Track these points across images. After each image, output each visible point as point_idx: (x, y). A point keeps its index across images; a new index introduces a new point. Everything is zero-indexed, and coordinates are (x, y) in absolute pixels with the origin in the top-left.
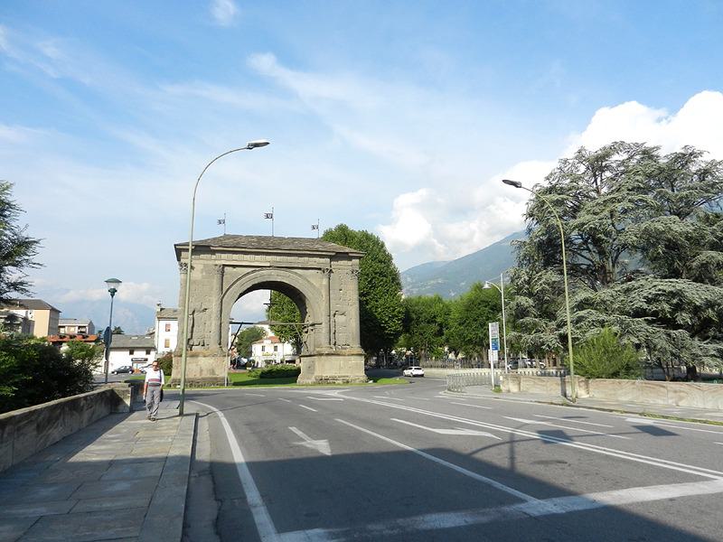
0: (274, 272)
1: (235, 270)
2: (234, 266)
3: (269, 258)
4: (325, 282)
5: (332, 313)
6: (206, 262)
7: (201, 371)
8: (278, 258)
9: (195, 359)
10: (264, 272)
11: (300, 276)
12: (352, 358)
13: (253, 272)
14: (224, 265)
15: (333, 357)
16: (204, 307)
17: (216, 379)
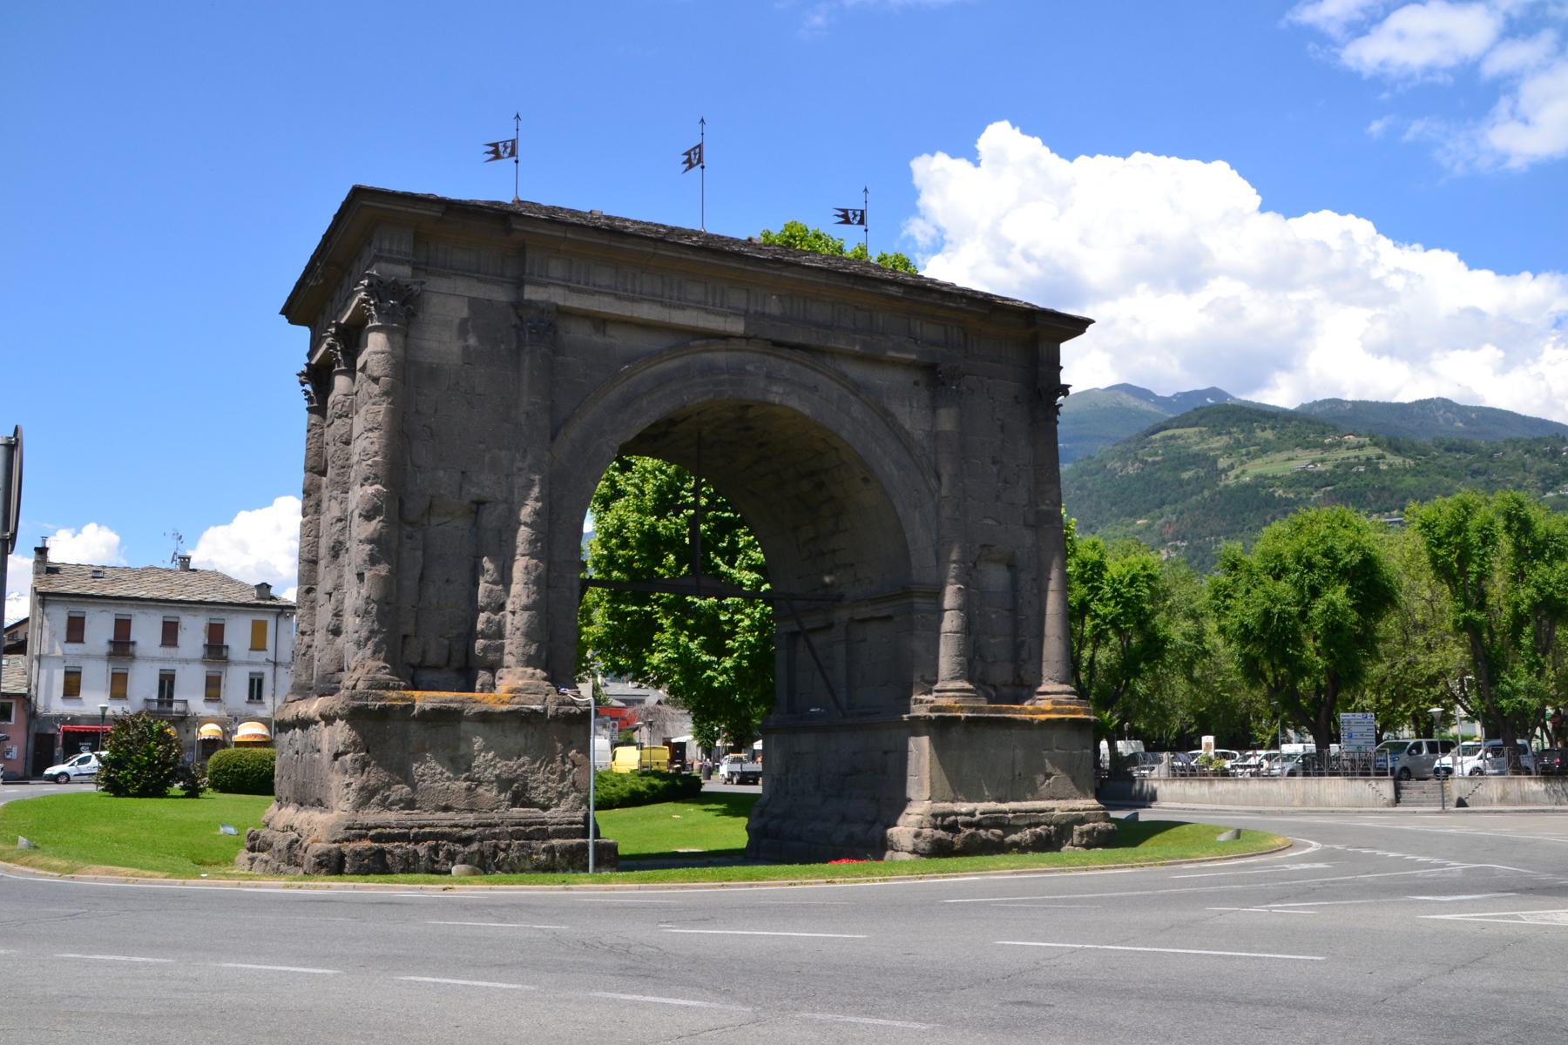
2: (601, 322)
3: (737, 298)
6: (482, 291)
10: (720, 357)
11: (857, 388)
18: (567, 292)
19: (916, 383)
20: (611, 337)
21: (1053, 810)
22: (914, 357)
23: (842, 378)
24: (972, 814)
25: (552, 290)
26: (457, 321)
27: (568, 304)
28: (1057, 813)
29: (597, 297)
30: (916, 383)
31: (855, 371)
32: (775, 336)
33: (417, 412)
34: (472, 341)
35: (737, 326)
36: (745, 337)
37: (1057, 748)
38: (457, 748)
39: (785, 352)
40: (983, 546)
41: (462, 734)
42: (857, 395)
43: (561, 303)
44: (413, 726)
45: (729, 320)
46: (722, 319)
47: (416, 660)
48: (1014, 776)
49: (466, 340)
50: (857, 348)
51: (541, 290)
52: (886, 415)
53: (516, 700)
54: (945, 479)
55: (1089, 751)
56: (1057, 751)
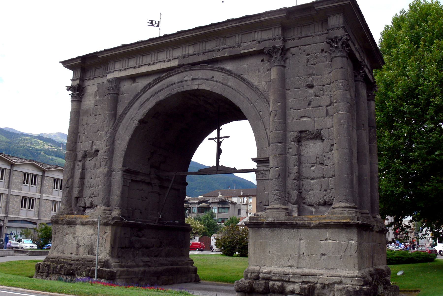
0: (188, 76)
1: (134, 85)
2: (133, 78)
3: (178, 53)
4: (274, 74)
5: (293, 135)
7: (78, 246)
8: (191, 50)
9: (71, 229)
10: (174, 79)
11: (229, 73)
12: (328, 233)
13: (156, 82)
14: (120, 80)
15: (285, 232)
16: (95, 147)
17: (92, 261)
18: (119, 72)
19: (262, 61)
20: (138, 82)
21: (322, 275)
22: (255, 49)
23: (223, 70)
24: (269, 273)
25: (115, 73)
26: (94, 93)
27: (119, 76)
28: (325, 276)
29: (128, 70)
30: (262, 61)
31: (229, 66)
32: (190, 62)
33: (82, 125)
34: (98, 98)
35: (175, 63)
36: (179, 66)
37: (330, 240)
38: (75, 234)
39: (198, 67)
40: (301, 132)
41: (77, 230)
42: (231, 75)
43: (117, 76)
44: (65, 226)
45: (172, 62)
46: (169, 63)
47: (82, 205)
48: (299, 254)
49: (96, 98)
50: (226, 55)
51: (112, 74)
52: (244, 80)
53: (91, 217)
54: (271, 104)
55: (354, 242)
56: (330, 241)
